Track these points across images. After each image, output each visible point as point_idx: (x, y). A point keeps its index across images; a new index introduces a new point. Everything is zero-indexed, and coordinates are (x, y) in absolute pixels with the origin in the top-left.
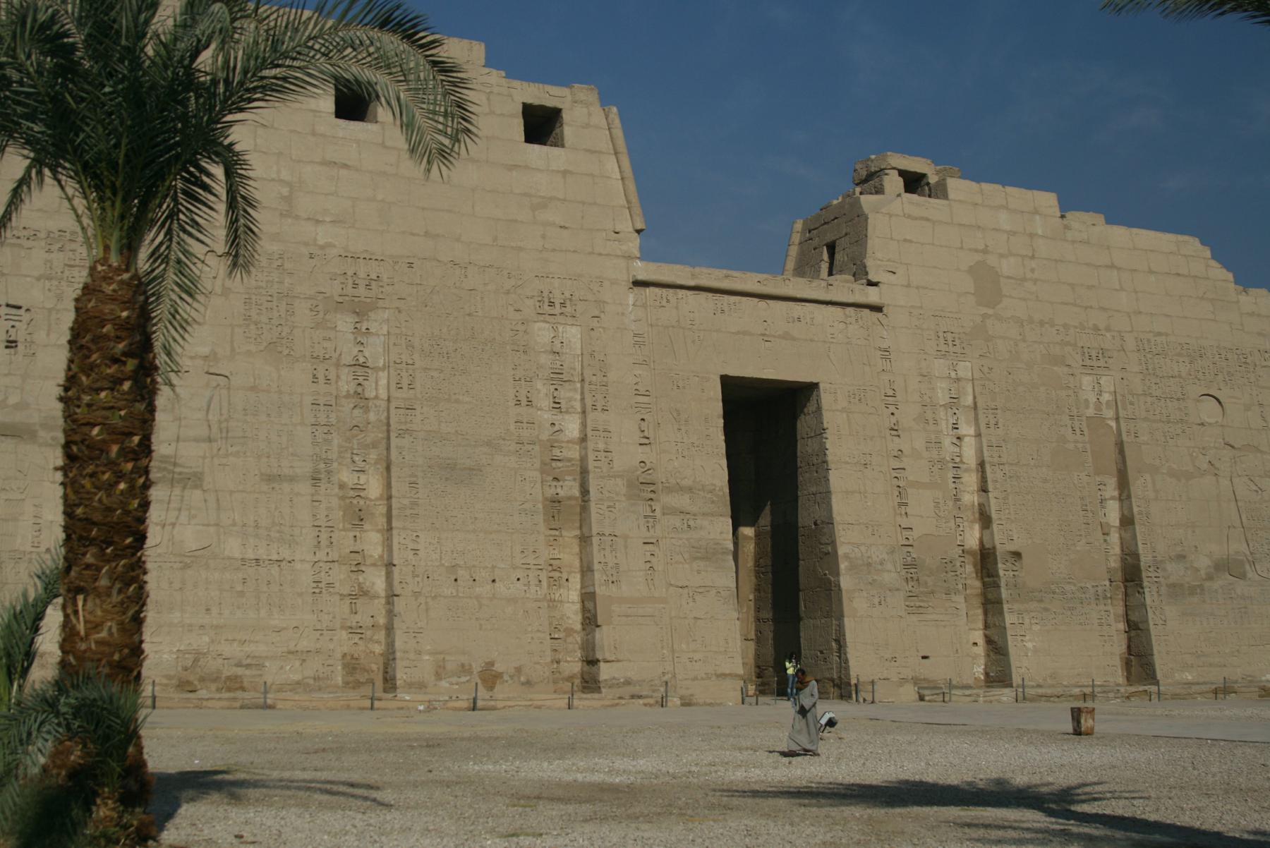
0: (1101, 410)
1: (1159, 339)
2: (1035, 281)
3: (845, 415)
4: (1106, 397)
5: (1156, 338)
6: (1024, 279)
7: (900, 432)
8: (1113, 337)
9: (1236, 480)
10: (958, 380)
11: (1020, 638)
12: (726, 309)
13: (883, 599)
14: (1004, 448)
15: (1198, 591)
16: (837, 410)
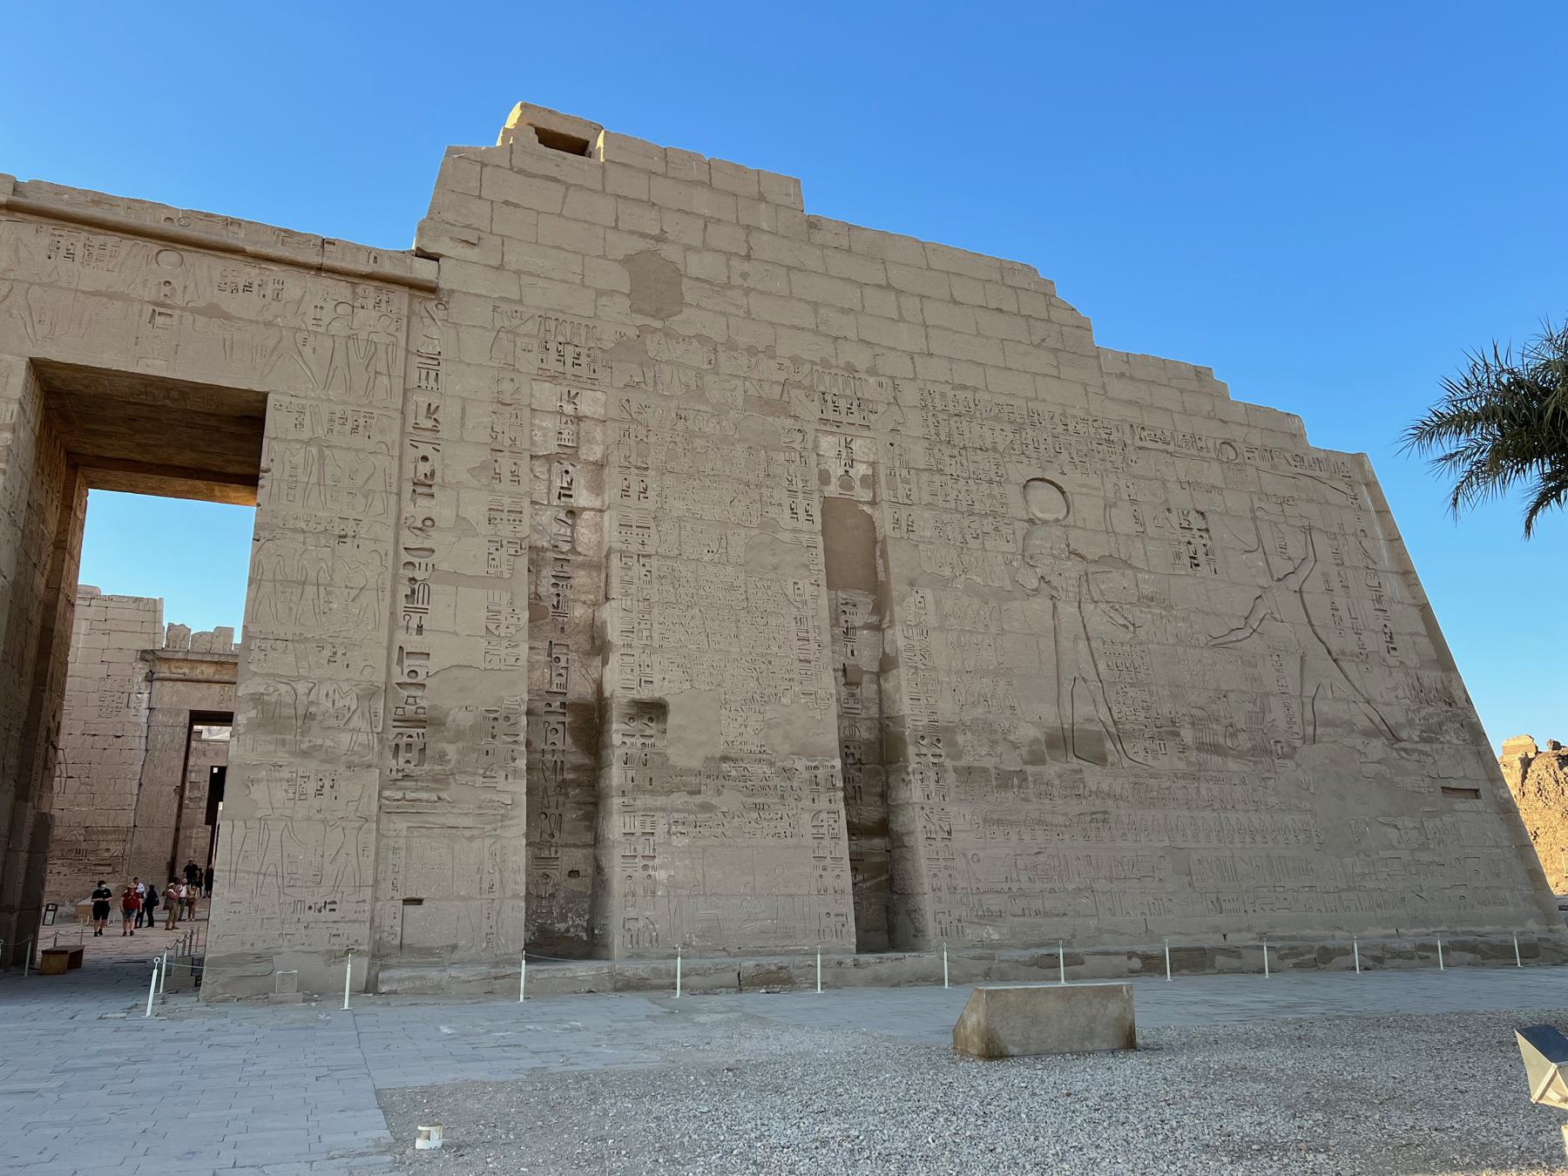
0: (852, 488)
1: (961, 394)
2: (748, 292)
3: (314, 450)
4: (861, 469)
5: (954, 392)
6: (728, 286)
7: (434, 490)
8: (880, 385)
9: (1088, 608)
10: (579, 419)
11: (640, 862)
12: (79, 251)
13: (328, 784)
14: (653, 531)
15: (1016, 782)
16: (297, 441)
